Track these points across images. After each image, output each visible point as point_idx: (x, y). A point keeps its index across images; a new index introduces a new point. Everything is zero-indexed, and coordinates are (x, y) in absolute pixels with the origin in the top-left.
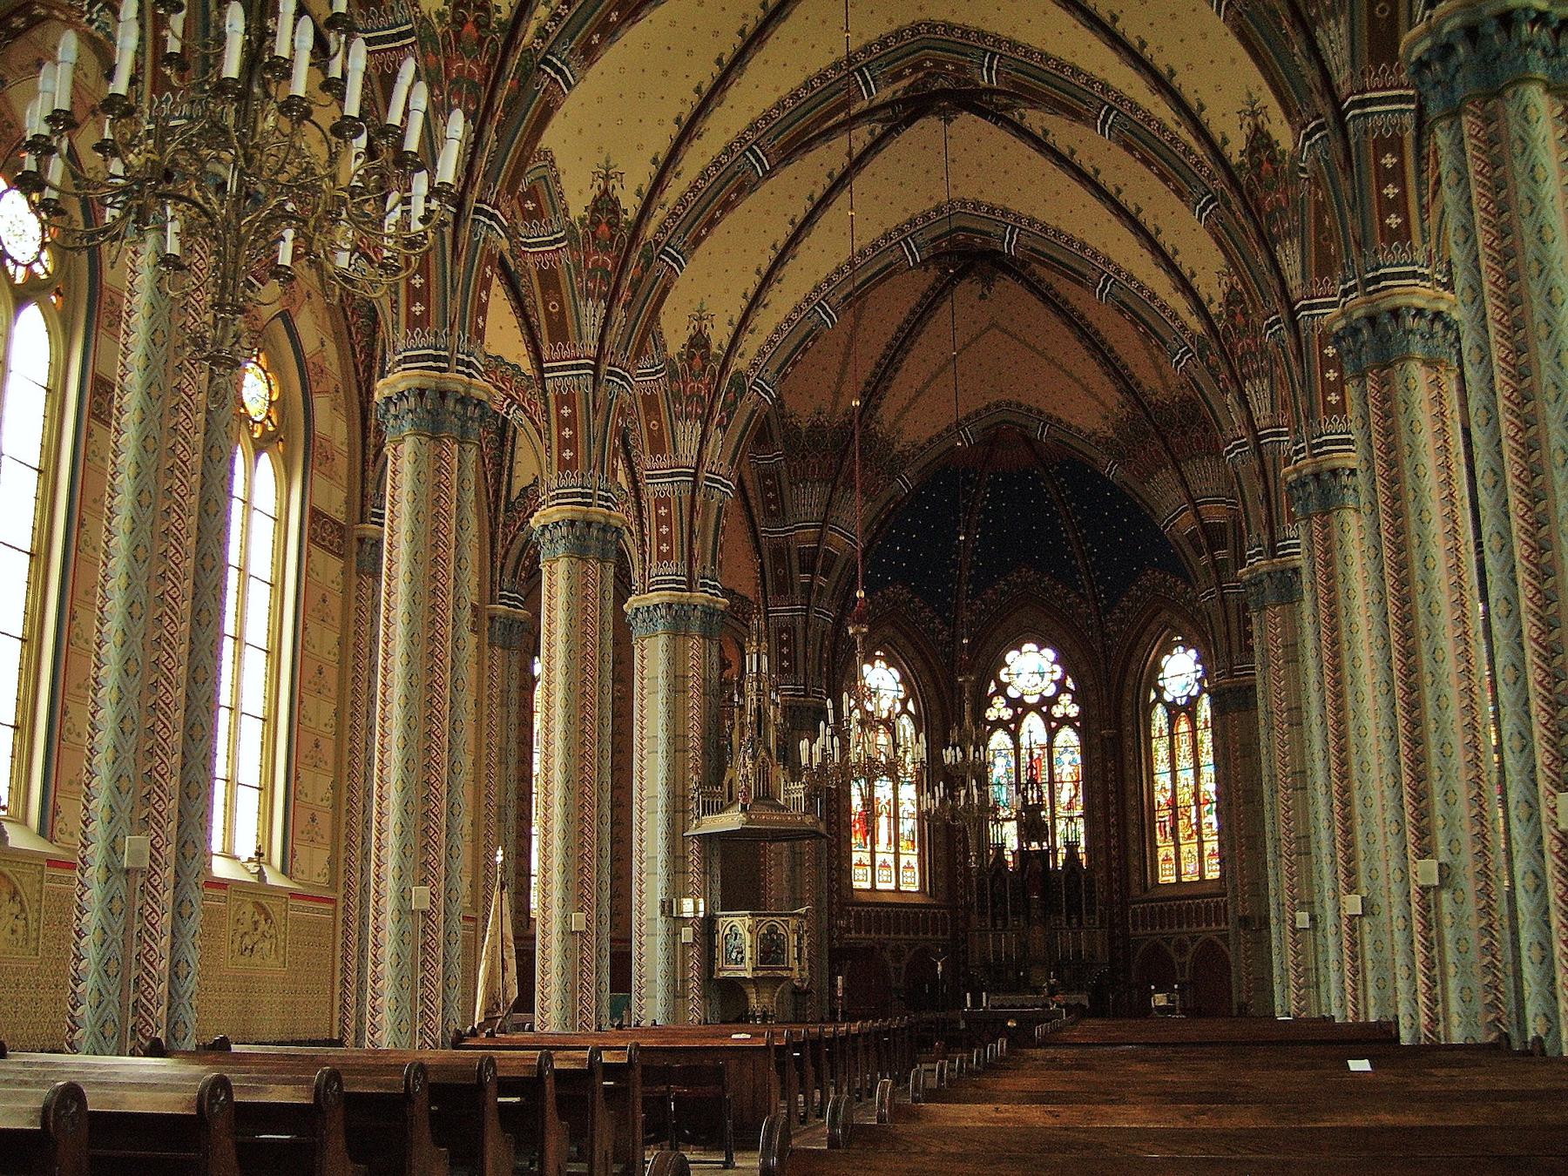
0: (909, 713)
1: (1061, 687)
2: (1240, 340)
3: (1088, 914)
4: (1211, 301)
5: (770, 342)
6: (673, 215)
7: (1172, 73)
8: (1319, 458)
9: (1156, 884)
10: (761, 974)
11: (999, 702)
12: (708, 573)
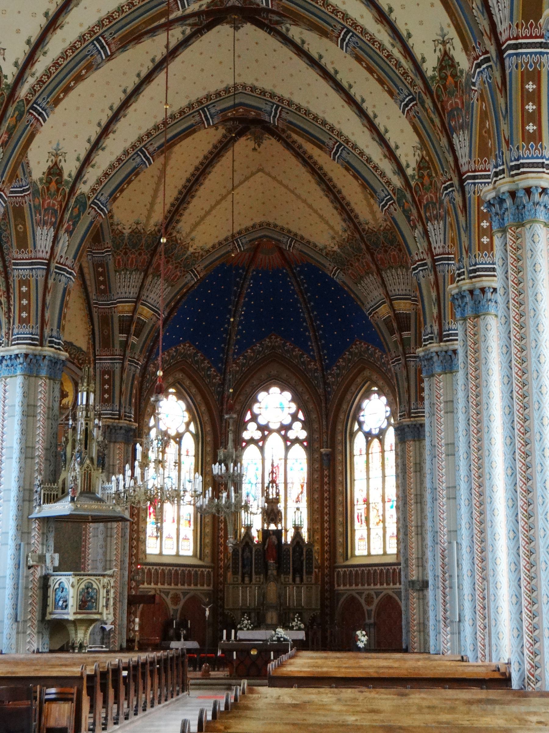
0: (191, 432)
1: (295, 417)
2: (426, 194)
3: (307, 573)
4: (408, 166)
5: (106, 174)
6: (40, 82)
7: (391, 10)
8: (474, 280)
9: (353, 555)
10: (79, 617)
11: (252, 426)
12: (55, 333)
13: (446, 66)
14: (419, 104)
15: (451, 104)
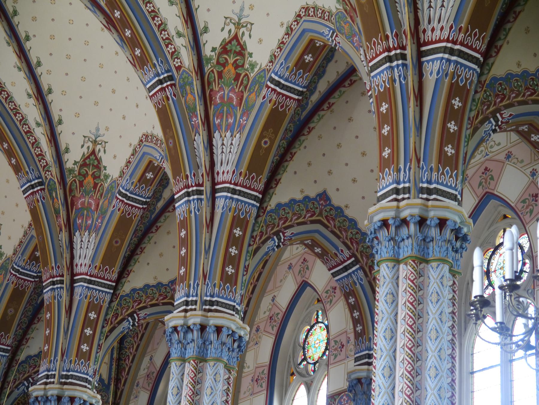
7: (50, 91)
8: (65, 387)
13: (90, 164)
14: (46, 190)
15: (83, 203)
